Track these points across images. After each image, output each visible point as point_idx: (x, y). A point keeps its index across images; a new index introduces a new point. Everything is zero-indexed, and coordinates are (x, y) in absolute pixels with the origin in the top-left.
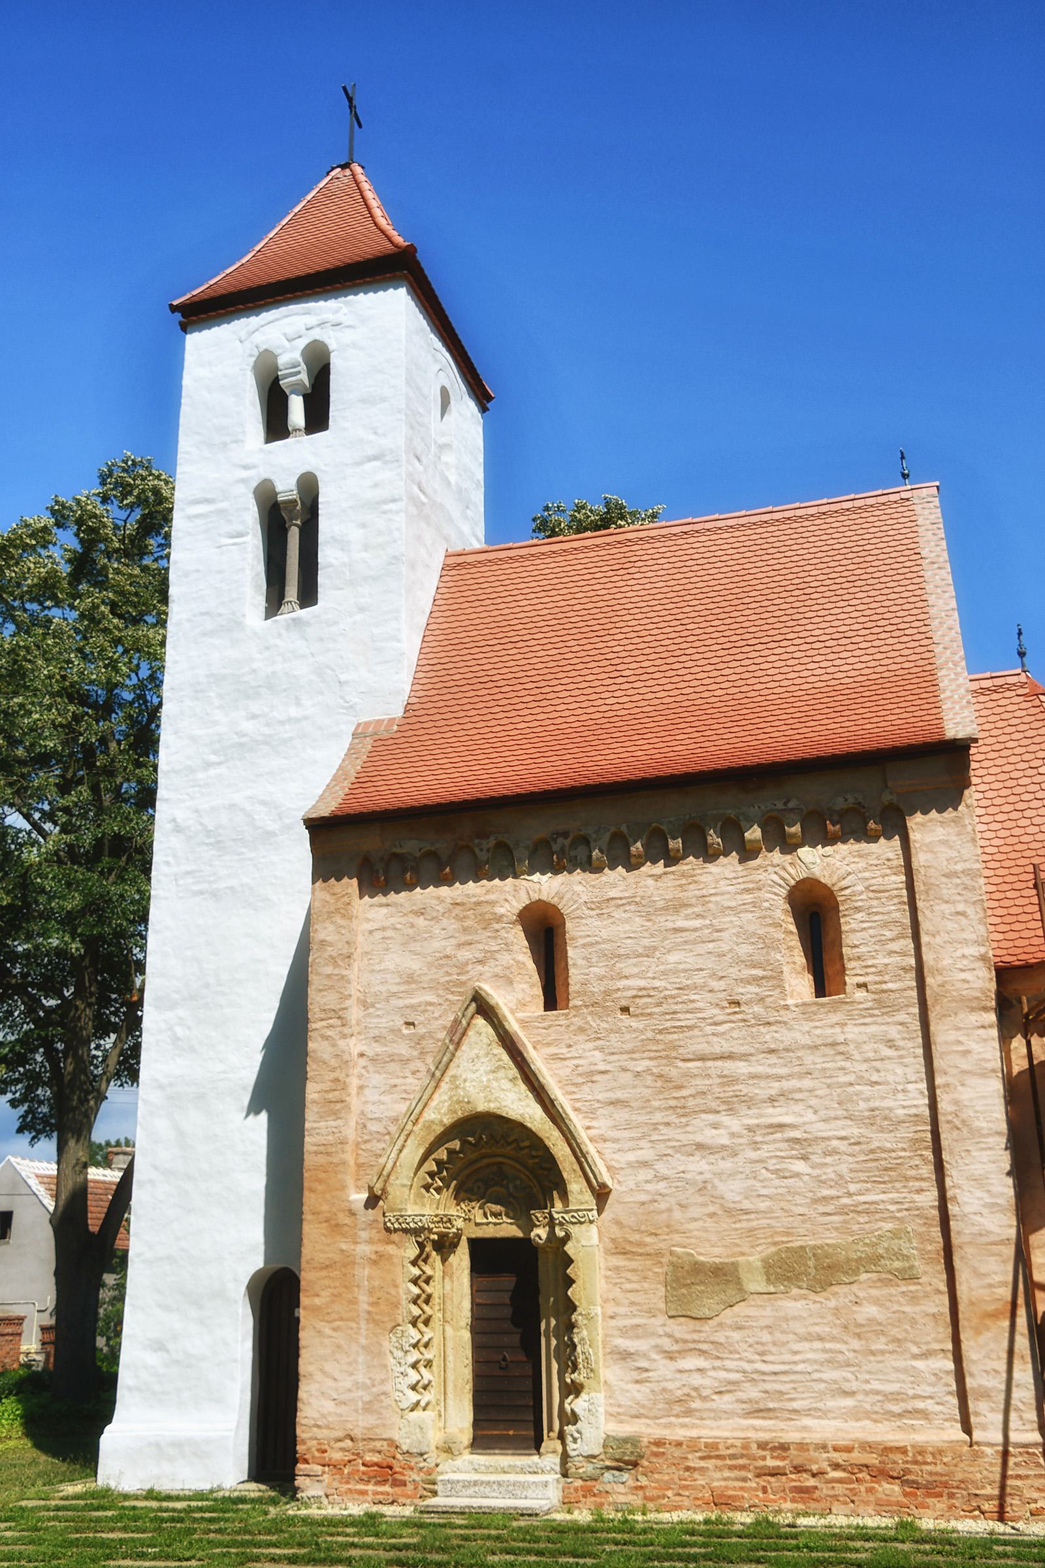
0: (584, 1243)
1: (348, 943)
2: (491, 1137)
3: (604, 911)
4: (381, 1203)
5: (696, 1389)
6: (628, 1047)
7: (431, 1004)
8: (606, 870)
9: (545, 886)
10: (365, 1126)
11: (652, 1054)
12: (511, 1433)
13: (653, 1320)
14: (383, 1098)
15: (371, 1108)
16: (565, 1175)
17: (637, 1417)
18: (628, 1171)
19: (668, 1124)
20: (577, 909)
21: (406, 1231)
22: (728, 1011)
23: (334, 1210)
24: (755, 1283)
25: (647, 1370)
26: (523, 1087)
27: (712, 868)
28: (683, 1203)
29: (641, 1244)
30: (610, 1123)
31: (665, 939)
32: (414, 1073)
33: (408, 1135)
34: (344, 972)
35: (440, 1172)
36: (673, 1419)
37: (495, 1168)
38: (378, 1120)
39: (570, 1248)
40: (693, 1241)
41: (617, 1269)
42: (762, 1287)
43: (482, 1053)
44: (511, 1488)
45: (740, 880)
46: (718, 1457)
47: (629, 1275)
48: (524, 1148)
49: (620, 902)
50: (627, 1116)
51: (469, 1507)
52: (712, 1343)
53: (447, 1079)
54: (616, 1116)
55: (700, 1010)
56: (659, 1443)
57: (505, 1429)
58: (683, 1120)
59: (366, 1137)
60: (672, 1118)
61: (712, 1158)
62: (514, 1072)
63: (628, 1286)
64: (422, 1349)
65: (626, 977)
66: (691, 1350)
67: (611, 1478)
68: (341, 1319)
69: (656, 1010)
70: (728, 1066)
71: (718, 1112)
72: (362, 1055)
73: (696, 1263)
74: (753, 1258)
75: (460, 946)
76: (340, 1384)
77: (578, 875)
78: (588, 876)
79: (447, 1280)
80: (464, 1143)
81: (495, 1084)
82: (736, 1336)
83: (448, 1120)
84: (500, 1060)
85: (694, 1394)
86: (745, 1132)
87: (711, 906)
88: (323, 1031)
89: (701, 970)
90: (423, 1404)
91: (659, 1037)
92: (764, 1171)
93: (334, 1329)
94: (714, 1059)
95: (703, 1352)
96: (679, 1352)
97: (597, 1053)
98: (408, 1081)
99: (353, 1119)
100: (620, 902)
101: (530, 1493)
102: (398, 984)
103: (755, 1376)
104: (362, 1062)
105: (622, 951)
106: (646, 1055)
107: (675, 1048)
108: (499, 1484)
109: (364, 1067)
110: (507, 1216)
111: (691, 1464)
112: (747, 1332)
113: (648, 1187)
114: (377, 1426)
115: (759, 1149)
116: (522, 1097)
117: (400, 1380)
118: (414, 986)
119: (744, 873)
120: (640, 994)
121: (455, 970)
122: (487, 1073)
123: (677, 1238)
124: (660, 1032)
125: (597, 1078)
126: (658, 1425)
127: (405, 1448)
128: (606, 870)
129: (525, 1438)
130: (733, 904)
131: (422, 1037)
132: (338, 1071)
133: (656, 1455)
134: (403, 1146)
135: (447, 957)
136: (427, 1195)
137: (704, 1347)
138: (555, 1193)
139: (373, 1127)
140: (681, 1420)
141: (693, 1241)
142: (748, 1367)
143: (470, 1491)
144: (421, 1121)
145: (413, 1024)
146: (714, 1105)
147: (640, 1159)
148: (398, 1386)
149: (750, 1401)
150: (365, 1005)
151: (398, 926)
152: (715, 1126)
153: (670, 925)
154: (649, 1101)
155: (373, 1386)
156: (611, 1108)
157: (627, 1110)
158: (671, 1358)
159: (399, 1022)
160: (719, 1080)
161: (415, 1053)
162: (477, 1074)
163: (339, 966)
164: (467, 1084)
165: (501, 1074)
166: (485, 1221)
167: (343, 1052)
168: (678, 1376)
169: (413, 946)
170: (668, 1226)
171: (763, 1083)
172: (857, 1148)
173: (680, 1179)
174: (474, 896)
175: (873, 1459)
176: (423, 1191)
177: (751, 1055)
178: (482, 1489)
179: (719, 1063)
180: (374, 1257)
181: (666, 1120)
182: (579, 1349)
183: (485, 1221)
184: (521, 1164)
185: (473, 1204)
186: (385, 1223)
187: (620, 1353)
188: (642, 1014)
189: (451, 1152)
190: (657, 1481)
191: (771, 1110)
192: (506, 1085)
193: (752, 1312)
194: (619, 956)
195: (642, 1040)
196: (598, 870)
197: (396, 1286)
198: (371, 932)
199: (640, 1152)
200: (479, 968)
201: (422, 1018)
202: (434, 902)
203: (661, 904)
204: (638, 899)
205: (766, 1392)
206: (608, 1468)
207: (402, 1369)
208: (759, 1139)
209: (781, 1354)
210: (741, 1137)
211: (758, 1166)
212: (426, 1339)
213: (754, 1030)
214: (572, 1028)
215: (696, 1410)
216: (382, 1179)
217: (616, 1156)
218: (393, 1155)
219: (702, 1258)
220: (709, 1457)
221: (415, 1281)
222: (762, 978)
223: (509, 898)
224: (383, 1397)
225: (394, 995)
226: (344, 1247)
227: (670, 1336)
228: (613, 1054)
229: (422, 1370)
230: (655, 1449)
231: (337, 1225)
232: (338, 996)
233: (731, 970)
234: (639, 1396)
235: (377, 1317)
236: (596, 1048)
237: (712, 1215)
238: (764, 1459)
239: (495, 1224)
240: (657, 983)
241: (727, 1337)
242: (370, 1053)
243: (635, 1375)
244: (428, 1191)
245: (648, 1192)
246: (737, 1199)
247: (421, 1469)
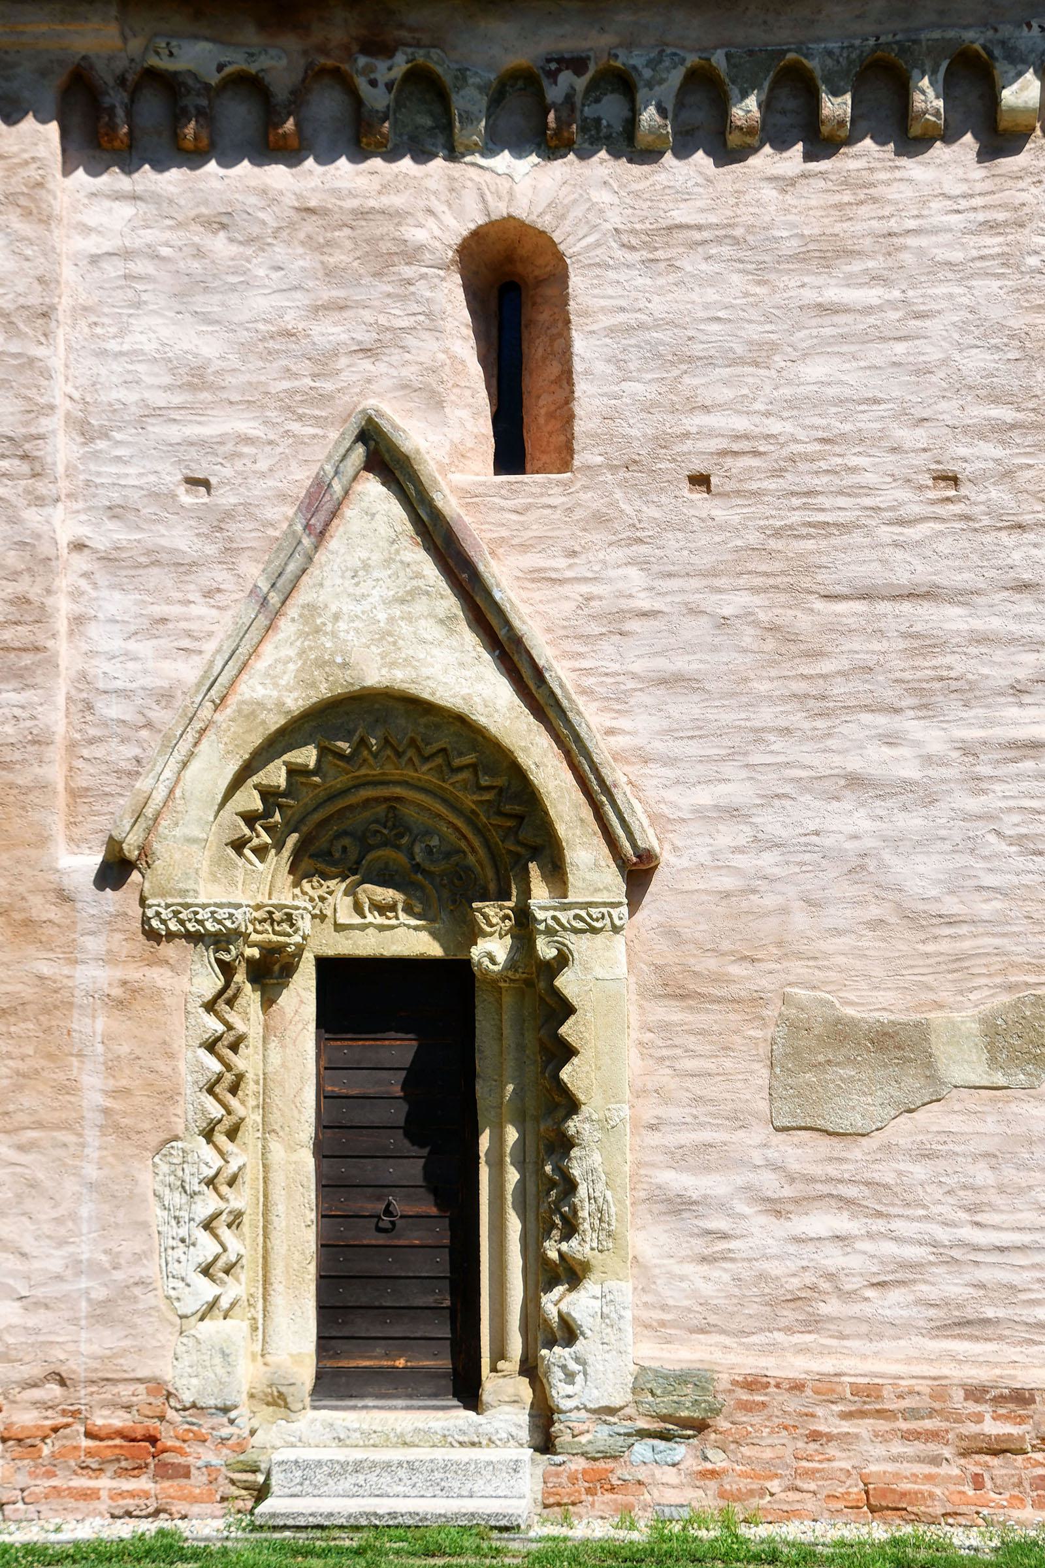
0: (600, 972)
1: (40, 280)
2: (387, 742)
3: (660, 254)
4: (135, 876)
5: (830, 1277)
6: (705, 561)
7: (248, 440)
8: (668, 158)
9: (523, 188)
10: (89, 707)
11: (758, 581)
12: (401, 1363)
13: (741, 1134)
14: (132, 645)
15: (106, 666)
16: (561, 830)
17: (702, 1331)
18: (695, 827)
19: (786, 731)
20: (598, 244)
21: (194, 938)
22: (932, 495)
23: (21, 889)
25: (725, 1236)
26: (470, 639)
27: (916, 169)
28: (817, 895)
29: (719, 979)
30: (656, 723)
31: (798, 327)
32: (208, 594)
33: (202, 732)
34: (39, 352)
35: (267, 814)
36: (779, 1336)
37: (381, 809)
38: (120, 693)
39: (566, 982)
40: (832, 975)
41: (665, 1027)
42: (978, 1073)
43: (376, 557)
44: (437, 1475)
45: (978, 201)
46: (880, 1414)
47: (691, 1041)
48: (460, 769)
49: (697, 236)
50: (696, 711)
51: (367, 1515)
52: (867, 1184)
53: (292, 610)
54: (674, 710)
55: (869, 490)
56: (753, 1384)
57: (387, 1356)
58: (821, 724)
59: (93, 732)
60: (797, 719)
61: (880, 807)
62: (450, 603)
63: (690, 1064)
64: (224, 1189)
65: (706, 409)
66: (821, 1197)
67: (649, 1455)
68: (40, 1125)
69: (771, 484)
70: (926, 616)
71: (897, 711)
72: (79, 546)
73: (838, 1021)
75: (318, 310)
76: (36, 1265)
77: (602, 165)
78: (624, 167)
79: (273, 1044)
80: (323, 752)
81: (405, 628)
82: (920, 1171)
83: (296, 702)
84: (418, 576)
85: (825, 1286)
86: (955, 754)
87: (907, 258)
89: (876, 401)
90: (224, 1303)
91: (773, 544)
92: (992, 838)
93: (21, 1148)
94: (894, 598)
95: (847, 1203)
96: (796, 1201)
97: (633, 572)
98: (196, 610)
99: (62, 688)
100: (697, 236)
101: (479, 1486)
102: (168, 388)
103: (956, 1253)
104: (80, 562)
105: (697, 349)
106: (742, 581)
107: (808, 570)
108: (411, 1466)
109: (86, 575)
110: (408, 910)
111: (823, 1428)
112: (942, 1164)
113: (740, 861)
114: (124, 1352)
115: (984, 792)
116: (468, 659)
117: (179, 1253)
118: (205, 396)
119: (988, 185)
120: (735, 447)
121: (305, 367)
122: (388, 603)
123: (799, 969)
124: (778, 533)
125: (633, 625)
126: (748, 1347)
127: (187, 1398)
128: (668, 158)
129: (431, 1375)
130: (957, 256)
131: (229, 515)
132: (26, 577)
133: (746, 1407)
134: (192, 754)
135: (289, 334)
136: (241, 862)
137: (851, 1191)
138: (533, 867)
139: (113, 710)
140: (798, 1338)
141: (832, 975)
142: (943, 1234)
143: (346, 1484)
144: (232, 701)
145: (205, 484)
146: (890, 695)
147: (723, 802)
148: (174, 1268)
149: (946, 1303)
150: (85, 431)
151: (165, 251)
152: (891, 740)
153: (809, 296)
154: (746, 680)
156: (661, 691)
157: (696, 698)
158: (778, 1213)
159: (172, 477)
160: (902, 644)
161: (211, 550)
162: (366, 605)
163: (20, 334)
164: (342, 625)
165: (420, 606)
166: (357, 920)
167: (39, 537)
168: (792, 1248)
169: (200, 302)
170: (780, 944)
171: (999, 655)
173: (808, 848)
174: (351, 194)
176: (230, 852)
177: (977, 592)
178: (372, 1477)
179: (906, 607)
180: (117, 992)
181: (782, 722)
182: (582, 1191)
183: (357, 920)
184: (445, 801)
185: (332, 883)
186: (145, 920)
187: (669, 1201)
188: (738, 493)
189: (294, 772)
190: (749, 1461)
191: (1014, 712)
192: (431, 630)
193: (955, 1123)
194: (691, 359)
195: (737, 550)
196: (647, 155)
197: (171, 1056)
198: (95, 260)
199: (723, 788)
200: (366, 365)
201: (228, 472)
202: (253, 200)
203: (792, 246)
204: (739, 232)
205: (982, 1286)
206: (643, 1434)
207: (183, 1232)
208: (984, 770)
209: (1016, 1210)
210: (943, 763)
211: (982, 827)
212: (233, 1167)
213: (988, 539)
214: (579, 514)
215: (831, 1319)
216: (142, 824)
217: (671, 795)
218: (168, 774)
219: (850, 1011)
220: (862, 1414)
221: (211, 1046)
222: (1013, 426)
223: (439, 207)
224: (137, 1291)
225: (157, 412)
226: (45, 969)
227: (775, 1167)
228: (670, 575)
229: (225, 1234)
230: (745, 1396)
231: (28, 923)
232: (20, 405)
233: (943, 405)
234: (707, 1289)
235: (125, 1121)
236: (631, 562)
238: (979, 1418)
239: (381, 928)
240: (775, 426)
241: (900, 1173)
242: (100, 543)
243: (699, 1246)
244: (240, 853)
245: (736, 871)
246: (933, 893)
247: (223, 1440)
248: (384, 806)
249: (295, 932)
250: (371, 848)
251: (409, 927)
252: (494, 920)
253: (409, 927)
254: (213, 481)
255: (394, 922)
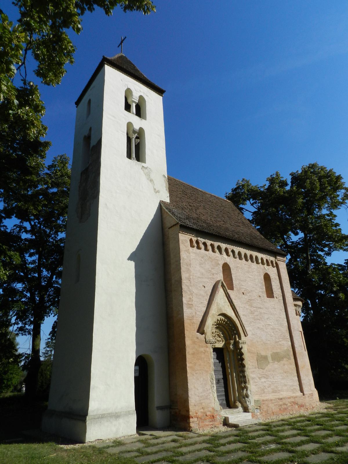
19: (253, 322)
24: (270, 359)
43: (222, 297)
56: (263, 400)
58: (255, 321)
60: (253, 320)
74: (269, 354)
88: (186, 283)
91: (249, 301)
96: (261, 377)
120: (245, 290)
121: (212, 275)
135: (210, 271)
137: (264, 376)
155: (207, 391)
161: (206, 294)
165: (226, 304)
172: (280, 331)
175: (293, 400)
186: (206, 341)
192: (227, 307)
194: (241, 280)
219: (262, 354)
225: (200, 277)
237: (262, 344)
240: (248, 289)
254: (205, 286)
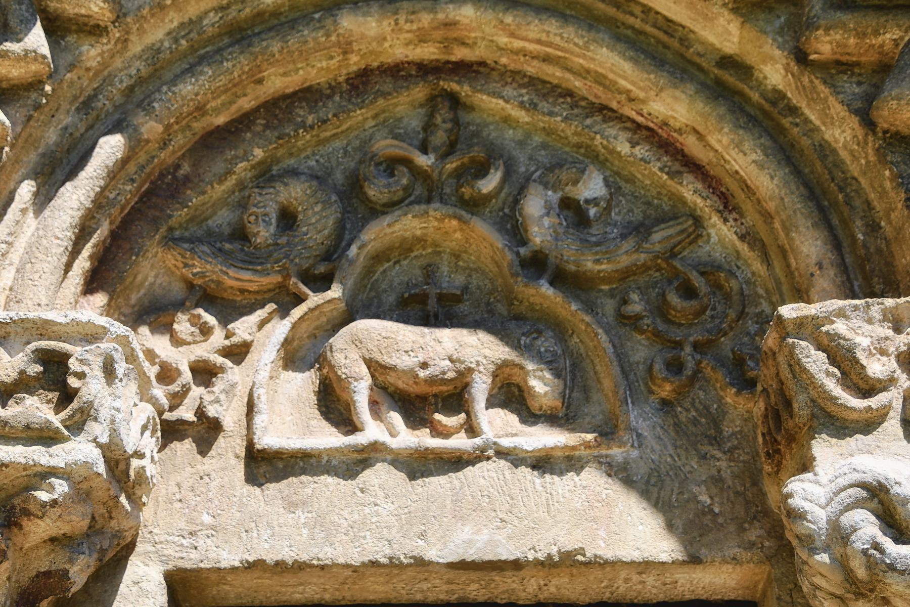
248: (419, 92)
249: (76, 426)
250: (375, 212)
251: (513, 457)
252: (876, 368)
253: (513, 457)
255: (460, 442)
